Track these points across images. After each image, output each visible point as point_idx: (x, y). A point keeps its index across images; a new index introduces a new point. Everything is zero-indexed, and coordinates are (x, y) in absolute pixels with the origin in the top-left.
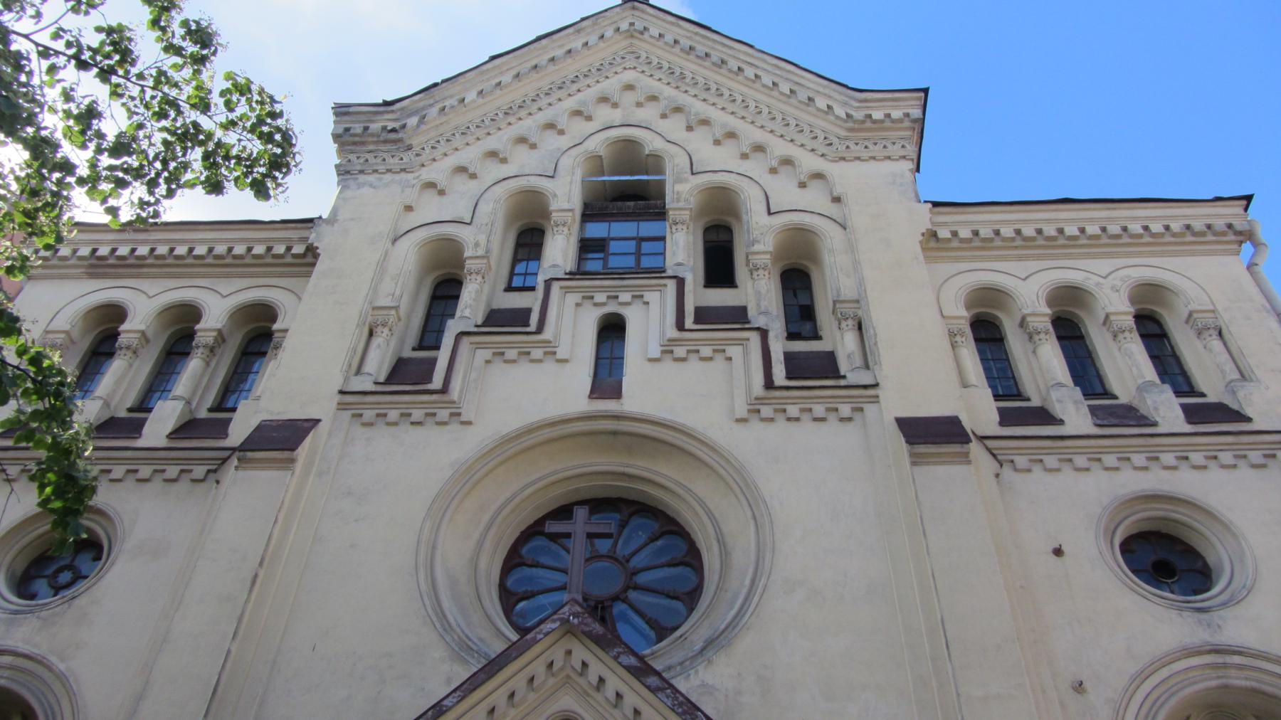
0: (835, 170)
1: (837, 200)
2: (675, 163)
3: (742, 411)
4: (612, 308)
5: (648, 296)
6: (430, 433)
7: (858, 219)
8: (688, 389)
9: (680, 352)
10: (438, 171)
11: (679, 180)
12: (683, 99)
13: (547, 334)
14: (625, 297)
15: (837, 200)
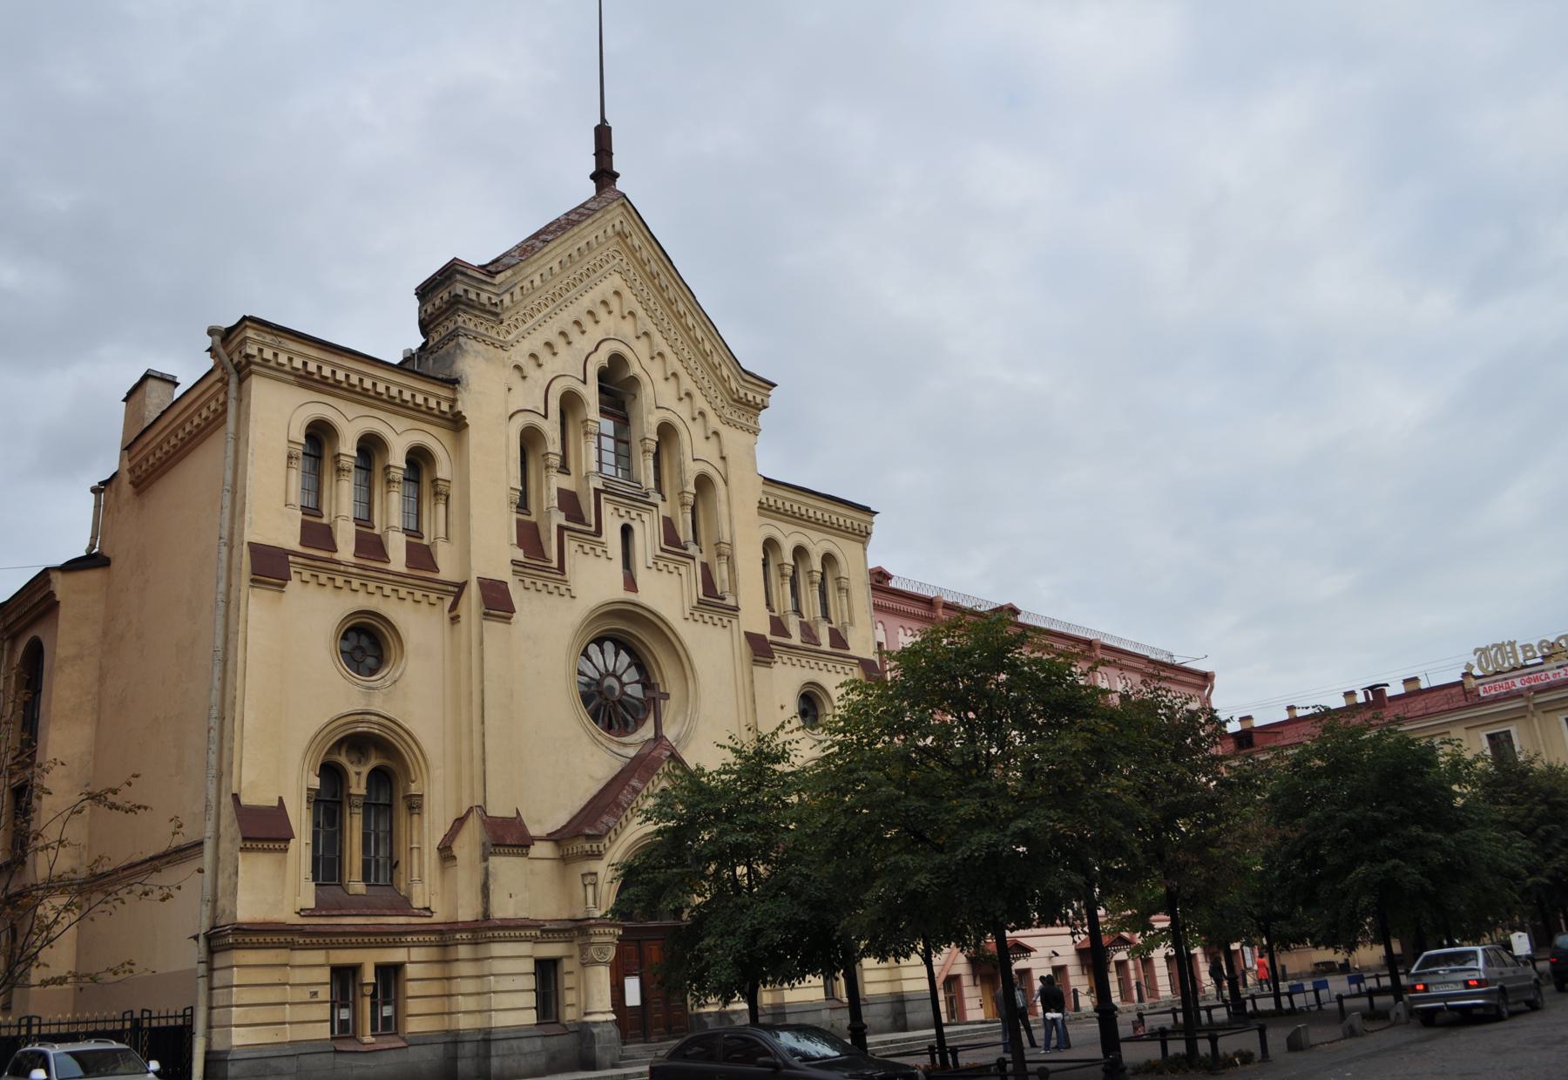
0: (725, 431)
1: (723, 458)
2: (647, 395)
3: (687, 612)
4: (626, 520)
5: (645, 517)
6: (555, 598)
7: (733, 480)
8: (666, 593)
9: (661, 564)
10: (519, 354)
11: (650, 412)
12: (652, 329)
13: (602, 539)
14: (634, 514)
15: (723, 458)
